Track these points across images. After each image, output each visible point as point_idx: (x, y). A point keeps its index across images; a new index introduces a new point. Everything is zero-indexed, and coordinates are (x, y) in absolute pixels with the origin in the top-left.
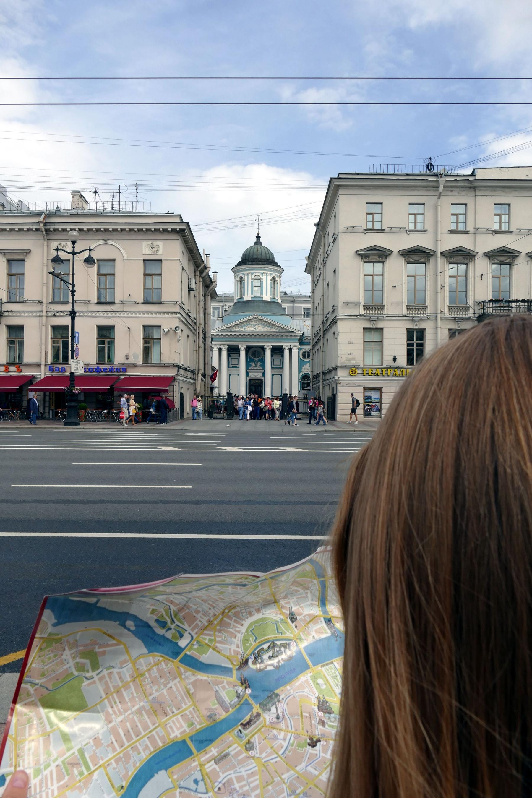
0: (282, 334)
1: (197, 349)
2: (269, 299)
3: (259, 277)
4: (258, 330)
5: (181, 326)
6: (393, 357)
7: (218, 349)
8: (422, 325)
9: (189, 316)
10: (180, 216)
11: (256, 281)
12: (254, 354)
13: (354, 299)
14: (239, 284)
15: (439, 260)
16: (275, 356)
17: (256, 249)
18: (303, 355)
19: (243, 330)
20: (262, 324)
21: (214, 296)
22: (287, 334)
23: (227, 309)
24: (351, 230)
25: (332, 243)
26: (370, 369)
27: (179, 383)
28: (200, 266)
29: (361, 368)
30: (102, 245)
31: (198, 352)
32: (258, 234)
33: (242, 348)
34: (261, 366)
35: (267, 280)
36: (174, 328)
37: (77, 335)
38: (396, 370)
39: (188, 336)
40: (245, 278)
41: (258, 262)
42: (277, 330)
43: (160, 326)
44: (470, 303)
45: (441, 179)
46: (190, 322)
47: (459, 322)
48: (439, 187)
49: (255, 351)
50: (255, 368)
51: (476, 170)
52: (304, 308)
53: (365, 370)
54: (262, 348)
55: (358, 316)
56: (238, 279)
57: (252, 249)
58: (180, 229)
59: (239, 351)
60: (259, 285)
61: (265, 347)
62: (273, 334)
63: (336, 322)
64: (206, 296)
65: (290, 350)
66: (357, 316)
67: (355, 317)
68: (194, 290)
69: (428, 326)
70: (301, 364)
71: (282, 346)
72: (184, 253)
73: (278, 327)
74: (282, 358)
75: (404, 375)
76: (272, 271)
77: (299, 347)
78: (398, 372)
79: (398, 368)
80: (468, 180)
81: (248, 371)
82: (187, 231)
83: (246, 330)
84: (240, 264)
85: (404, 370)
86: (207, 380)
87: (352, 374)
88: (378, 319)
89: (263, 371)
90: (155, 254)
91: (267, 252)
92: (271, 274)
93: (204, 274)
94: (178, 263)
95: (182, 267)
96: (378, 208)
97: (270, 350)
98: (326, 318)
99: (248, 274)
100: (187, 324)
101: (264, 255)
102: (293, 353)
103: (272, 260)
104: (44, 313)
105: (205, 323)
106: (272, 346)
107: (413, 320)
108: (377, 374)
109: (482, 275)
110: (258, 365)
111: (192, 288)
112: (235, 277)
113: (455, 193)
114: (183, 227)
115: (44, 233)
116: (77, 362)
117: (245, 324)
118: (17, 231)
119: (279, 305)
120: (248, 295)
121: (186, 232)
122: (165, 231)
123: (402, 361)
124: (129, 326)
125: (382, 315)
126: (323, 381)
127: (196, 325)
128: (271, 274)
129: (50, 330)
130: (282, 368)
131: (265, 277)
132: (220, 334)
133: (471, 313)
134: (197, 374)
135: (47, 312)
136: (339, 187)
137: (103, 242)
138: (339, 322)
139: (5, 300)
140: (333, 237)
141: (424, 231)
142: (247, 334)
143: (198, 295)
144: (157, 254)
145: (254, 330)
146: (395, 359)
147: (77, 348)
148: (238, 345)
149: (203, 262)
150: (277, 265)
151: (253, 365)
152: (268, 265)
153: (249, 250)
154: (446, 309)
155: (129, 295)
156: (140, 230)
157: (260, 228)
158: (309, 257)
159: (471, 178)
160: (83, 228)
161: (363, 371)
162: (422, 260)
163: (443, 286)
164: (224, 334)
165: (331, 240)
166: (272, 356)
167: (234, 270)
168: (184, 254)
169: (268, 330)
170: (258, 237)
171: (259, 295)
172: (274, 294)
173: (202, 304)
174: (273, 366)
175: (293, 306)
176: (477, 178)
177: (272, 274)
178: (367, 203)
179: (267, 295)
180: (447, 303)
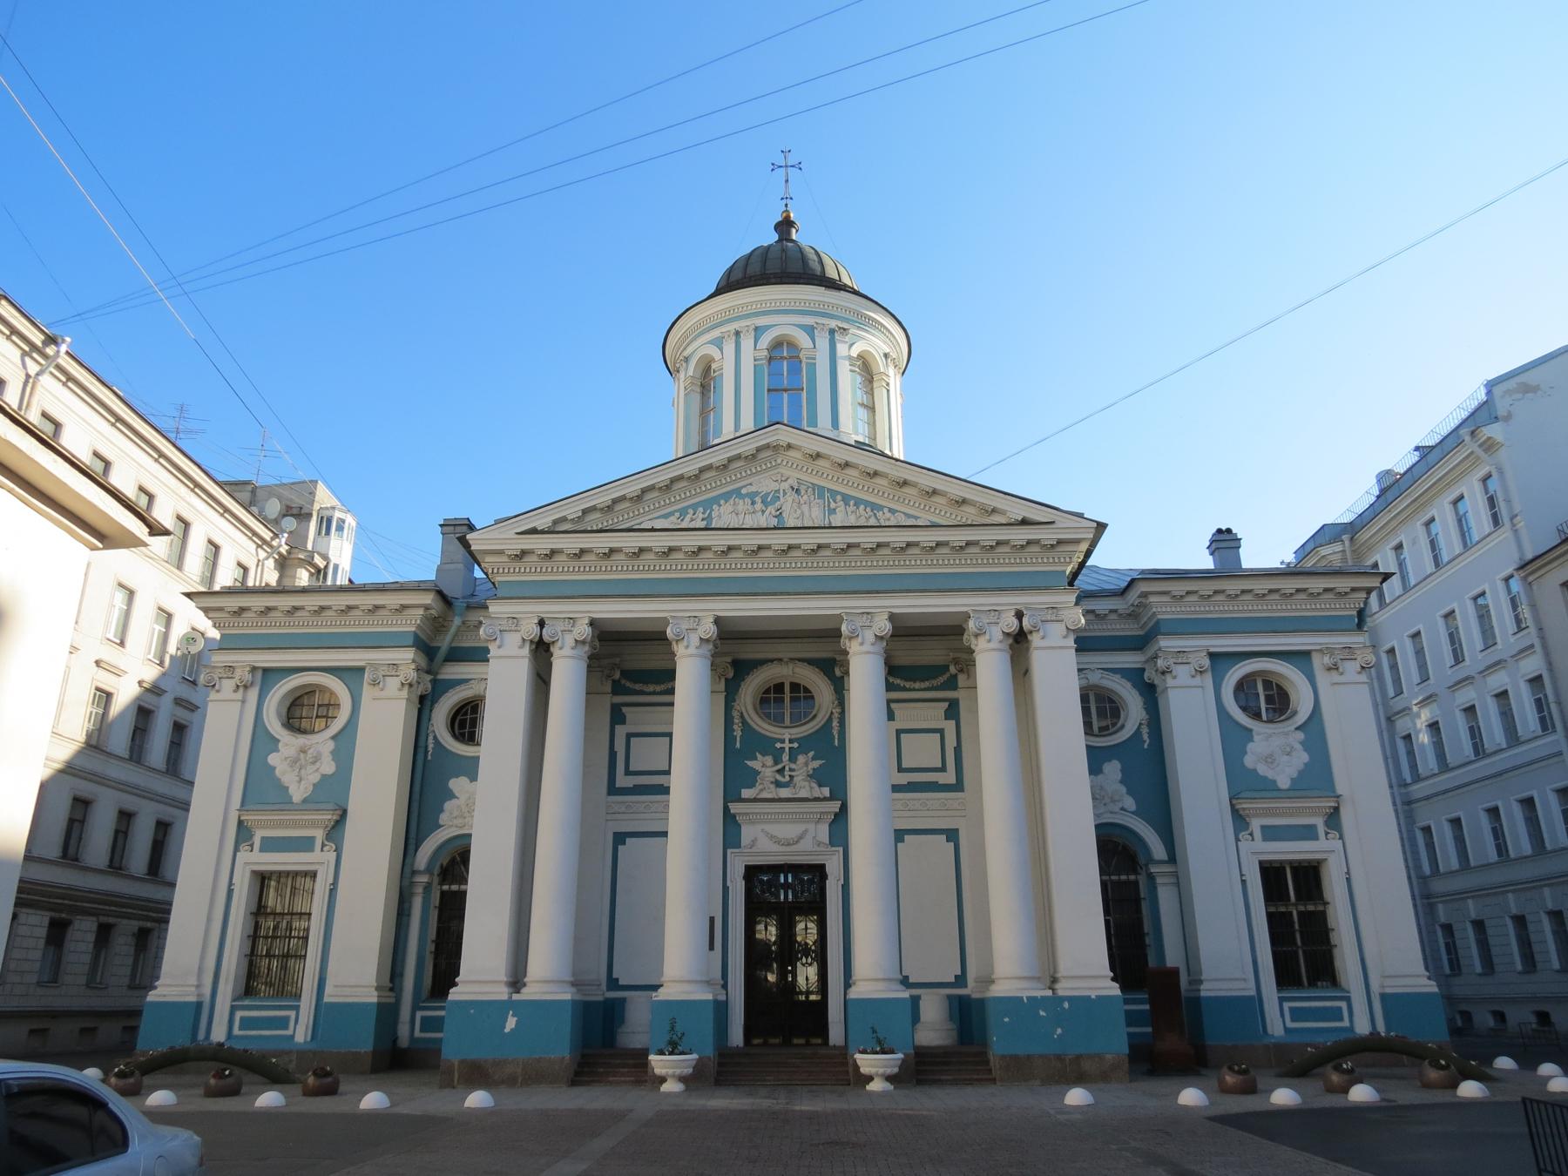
7: (526, 651)
14: (697, 398)
16: (910, 716)
34: (818, 777)
49: (779, 688)
50: (784, 793)
74: (949, 726)
81: (735, 808)
89: (835, 806)
99: (737, 333)
130: (958, 786)
132: (543, 544)
142: (719, 541)
169: (862, 522)
170: (785, 226)
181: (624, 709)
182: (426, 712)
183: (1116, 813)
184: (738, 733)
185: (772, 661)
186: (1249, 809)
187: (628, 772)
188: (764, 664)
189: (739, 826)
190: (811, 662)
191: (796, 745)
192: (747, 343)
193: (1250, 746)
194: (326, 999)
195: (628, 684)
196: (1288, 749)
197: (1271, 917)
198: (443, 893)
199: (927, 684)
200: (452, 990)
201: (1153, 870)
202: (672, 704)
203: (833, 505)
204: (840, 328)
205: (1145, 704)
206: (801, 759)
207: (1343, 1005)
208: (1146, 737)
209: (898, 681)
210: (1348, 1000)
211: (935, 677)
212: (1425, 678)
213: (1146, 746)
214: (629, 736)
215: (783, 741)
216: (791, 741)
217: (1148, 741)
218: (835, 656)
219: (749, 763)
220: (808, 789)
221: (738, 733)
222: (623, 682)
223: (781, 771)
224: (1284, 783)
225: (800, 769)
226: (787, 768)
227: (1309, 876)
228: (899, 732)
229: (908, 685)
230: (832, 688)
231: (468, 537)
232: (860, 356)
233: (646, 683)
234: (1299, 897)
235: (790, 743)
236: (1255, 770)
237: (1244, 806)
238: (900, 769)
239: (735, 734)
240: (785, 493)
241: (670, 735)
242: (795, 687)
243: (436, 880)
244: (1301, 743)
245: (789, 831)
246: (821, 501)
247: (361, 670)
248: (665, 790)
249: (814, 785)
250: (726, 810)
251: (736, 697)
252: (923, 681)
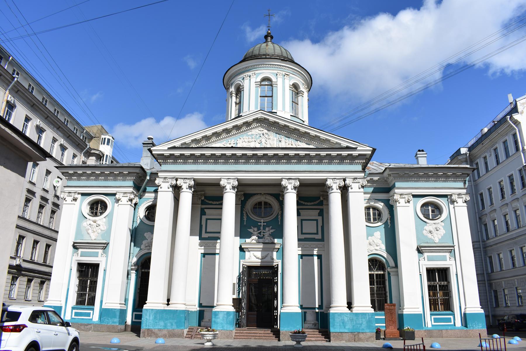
0: (323, 153)
7: (171, 189)
22: (334, 153)
33: (228, 187)
40: (246, 84)
49: (260, 203)
65: (344, 190)
74: (320, 219)
99: (250, 77)
110: (267, 234)
130: (322, 240)
132: (177, 153)
148: (220, 180)
164: (187, 153)
181: (205, 210)
182: (136, 210)
183: (377, 250)
184: (245, 219)
185: (258, 194)
186: (424, 250)
187: (206, 232)
188: (255, 195)
189: (245, 252)
190: (271, 195)
191: (265, 224)
192: (253, 80)
193: (426, 227)
194: (103, 307)
195: (207, 201)
196: (438, 229)
197: (429, 287)
198: (142, 272)
199: (312, 203)
200: (144, 306)
201: (389, 270)
202: (221, 208)
203: (280, 139)
204: (286, 74)
205: (389, 212)
206: (267, 229)
207: (452, 317)
208: (389, 223)
209: (302, 202)
210: (454, 315)
211: (315, 201)
212: (492, 204)
213: (389, 227)
214: (207, 219)
215: (261, 222)
216: (264, 223)
217: (390, 225)
218: (280, 193)
219: (249, 230)
220: (269, 239)
221: (245, 219)
222: (205, 200)
223: (260, 233)
224: (437, 240)
225: (267, 232)
226: (262, 232)
227: (444, 273)
228: (302, 220)
229: (306, 203)
230: (279, 204)
231: (151, 149)
232: (293, 84)
233: (213, 201)
234: (439, 280)
235: (263, 223)
236: (427, 236)
237: (422, 248)
238: (302, 233)
239: (244, 219)
240: (263, 134)
241: (221, 219)
242: (266, 203)
243: (140, 268)
244: (443, 227)
246: (276, 138)
247: (114, 194)
249: (272, 238)
250: (241, 246)
251: (245, 207)
252: (311, 202)
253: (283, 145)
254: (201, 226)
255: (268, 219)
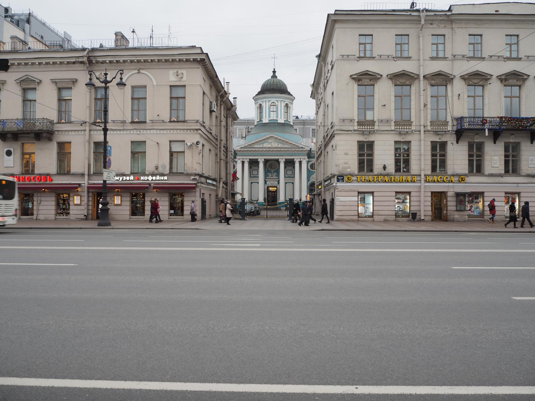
0: (293, 150)
1: (219, 161)
2: (283, 122)
3: (275, 104)
4: (274, 146)
5: (202, 141)
6: (383, 166)
8: (408, 138)
9: (211, 133)
10: (201, 48)
11: (272, 107)
12: (271, 166)
13: (348, 116)
14: (259, 110)
15: (422, 82)
16: (288, 168)
17: (272, 81)
18: (311, 166)
19: (262, 146)
20: (277, 142)
21: (235, 117)
22: (297, 150)
23: (250, 130)
24: (345, 57)
25: (330, 70)
26: (363, 177)
27: (200, 189)
28: (221, 91)
29: (355, 175)
30: (135, 74)
31: (219, 163)
32: (274, 69)
33: (261, 161)
34: (276, 176)
35: (281, 106)
36: (195, 143)
37: (109, 148)
38: (386, 177)
39: (210, 150)
40: (264, 105)
41: (274, 92)
42: (289, 147)
43: (184, 141)
44: (449, 119)
45: (421, 14)
46: (212, 138)
47: (440, 136)
48: (421, 21)
50: (272, 178)
51: (452, 7)
52: (312, 129)
53: (359, 177)
54: (278, 161)
55: (353, 131)
56: (258, 105)
57: (269, 82)
58: (200, 59)
59: (259, 164)
60: (275, 110)
61: (279, 160)
62: (286, 149)
63: (334, 137)
64: (228, 117)
65: (300, 162)
66: (351, 131)
67: (351, 132)
68: (215, 112)
69: (413, 138)
70: (309, 174)
71: (294, 159)
72: (205, 80)
73: (290, 143)
74: (293, 169)
75: (392, 181)
76: (286, 98)
77: (307, 160)
78: (387, 178)
79: (388, 175)
80: (446, 14)
81: (266, 180)
82: (207, 60)
83: (264, 146)
84: (259, 93)
85: (392, 177)
86: (228, 187)
87: (348, 180)
88: (370, 133)
89: (278, 180)
90: (180, 81)
91: (281, 83)
92: (284, 102)
93: (225, 98)
94: (199, 88)
95: (203, 91)
96: (368, 40)
97: (284, 163)
98: (327, 134)
99: (266, 101)
100: (209, 140)
101: (279, 86)
102: (302, 164)
103: (285, 90)
104: (87, 132)
105: (227, 140)
106: (285, 159)
107: (400, 133)
108: (369, 180)
109: (459, 95)
110: (274, 175)
111: (213, 109)
112: (255, 104)
113: (434, 26)
114: (203, 57)
115: (88, 65)
116: (109, 172)
117: (263, 142)
118: (66, 64)
119: (292, 126)
120: (266, 118)
121: (206, 62)
122: (187, 60)
123: (391, 169)
124: (157, 142)
125: (373, 130)
126: (324, 187)
127: (218, 141)
128: (284, 102)
129: (92, 145)
130: (294, 177)
131: (279, 103)
132: (243, 150)
133: (450, 128)
134: (218, 182)
135: (90, 130)
136: (335, 21)
137: (136, 71)
138: (335, 136)
139: (55, 121)
140: (331, 65)
141: (409, 58)
142: (264, 150)
143: (219, 116)
144: (182, 80)
145: (271, 146)
146: (385, 168)
147: (109, 159)
148: (258, 159)
149: (223, 88)
150: (289, 94)
151: (270, 175)
152: (282, 94)
153: (267, 82)
154: (429, 124)
155: (158, 115)
156: (166, 61)
157: (275, 64)
158: (313, 84)
159: (449, 13)
160: (120, 60)
161: (358, 178)
162: (408, 83)
163: (426, 104)
164: (246, 149)
165: (330, 67)
166: (285, 167)
167: (255, 99)
168: (205, 81)
170: (274, 72)
171: (275, 118)
172: (287, 118)
173: (224, 123)
174: (286, 176)
175: (303, 128)
176: (453, 12)
177: (285, 101)
178: (360, 35)
179: (281, 118)
180: (429, 118)
184: (266, 170)
221: (266, 170)
245: (272, 182)
248: (258, 177)
253: (280, 146)
254: (250, 172)
255: (274, 170)
